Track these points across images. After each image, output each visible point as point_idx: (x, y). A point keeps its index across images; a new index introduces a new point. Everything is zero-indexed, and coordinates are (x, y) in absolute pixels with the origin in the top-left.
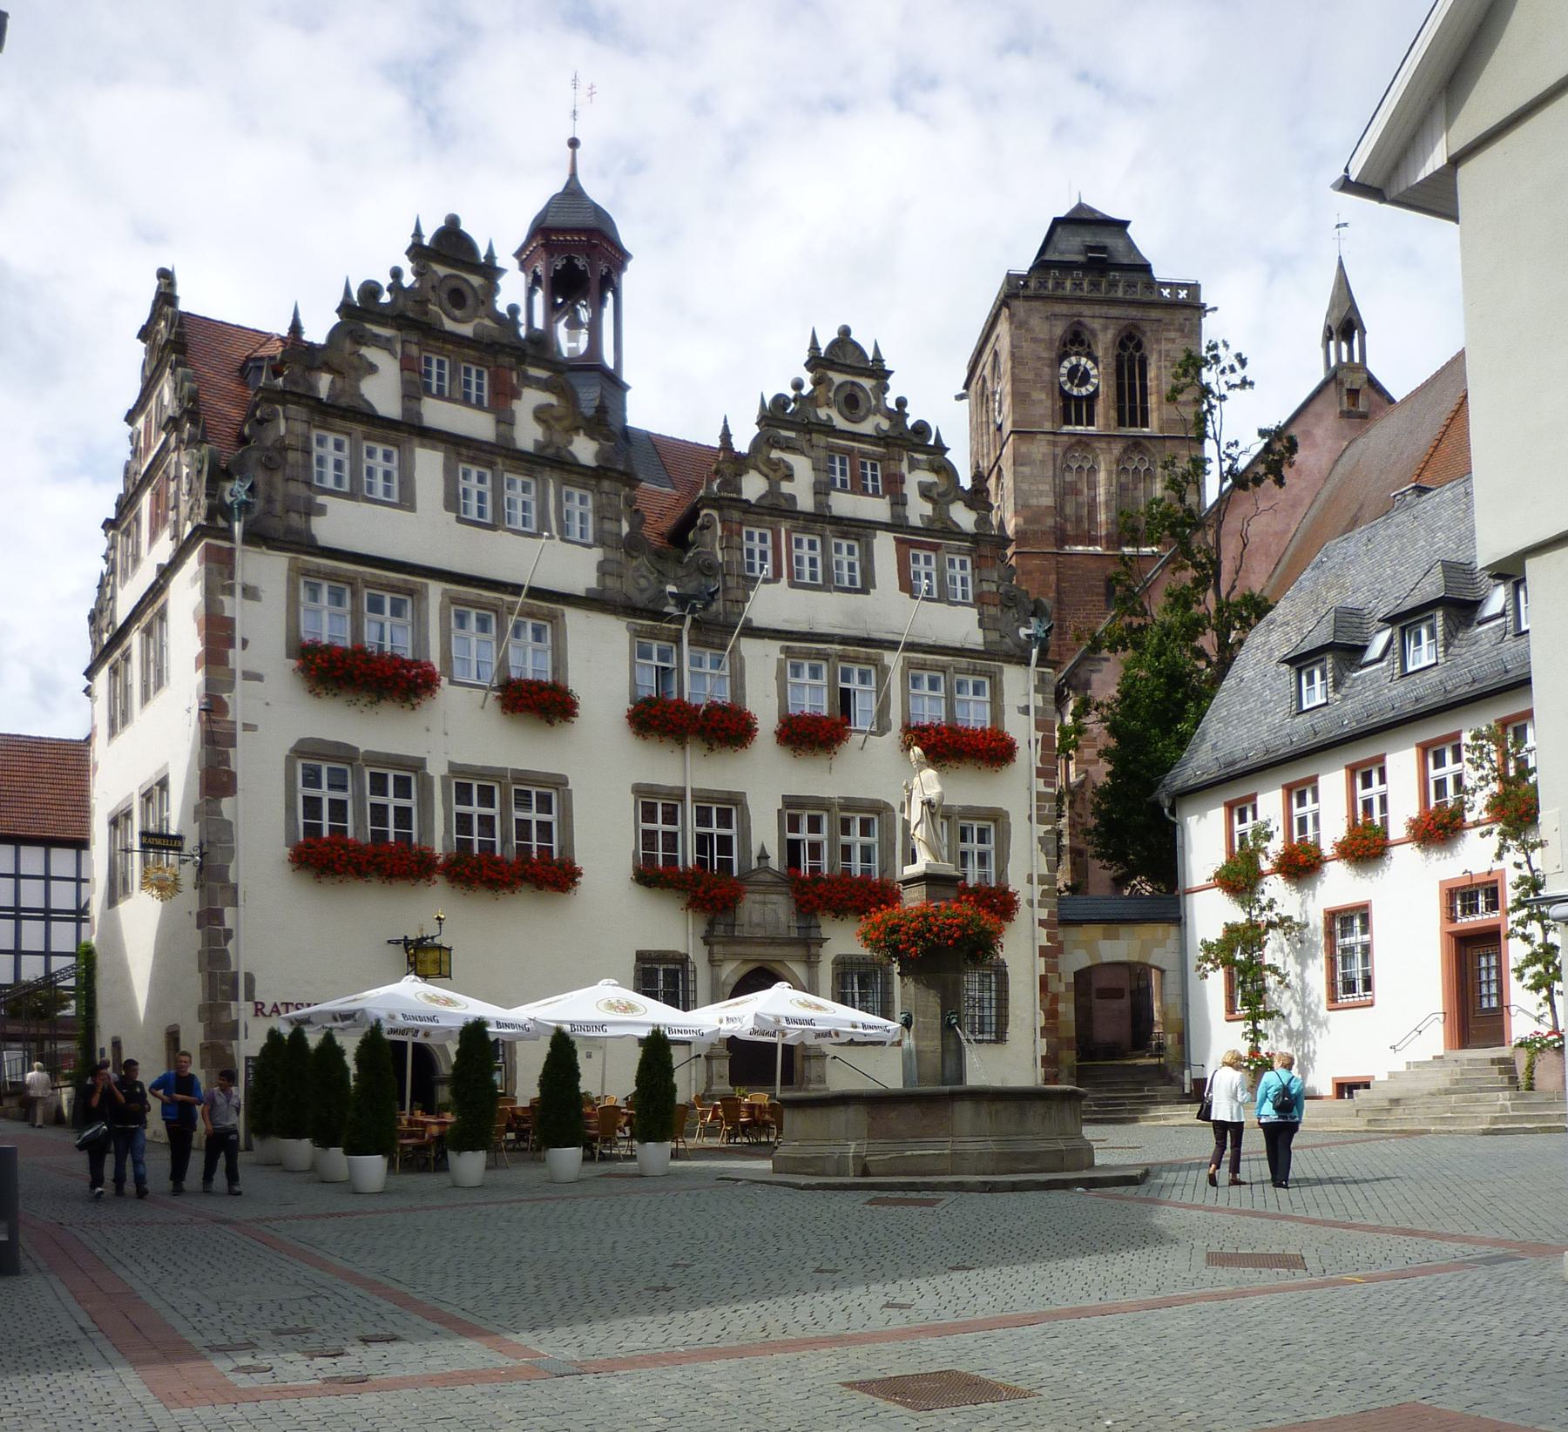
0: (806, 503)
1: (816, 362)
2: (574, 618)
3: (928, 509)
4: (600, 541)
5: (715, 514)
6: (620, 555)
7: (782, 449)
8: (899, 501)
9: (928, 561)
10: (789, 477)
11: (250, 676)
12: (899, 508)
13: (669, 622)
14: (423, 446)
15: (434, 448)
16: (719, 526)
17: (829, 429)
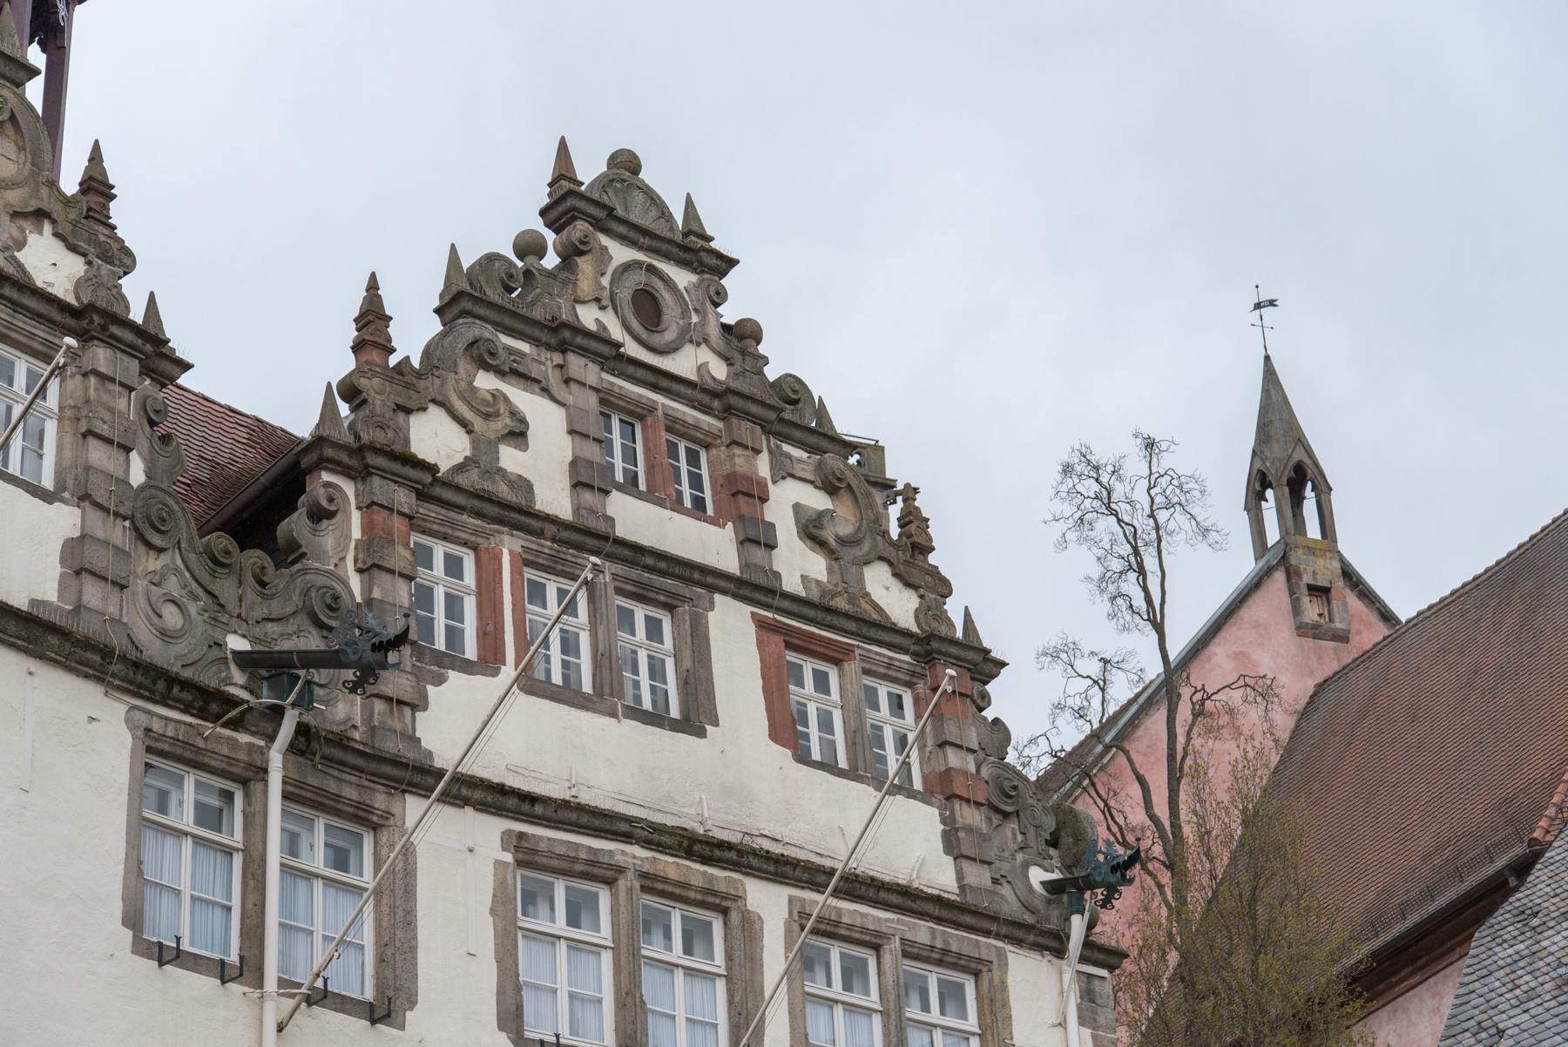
0: (555, 498)
1: (567, 204)
3: (817, 566)
4: (76, 488)
5: (348, 488)
6: (119, 533)
7: (500, 373)
8: (757, 538)
9: (822, 683)
10: (518, 435)
12: (758, 554)
13: (235, 724)
16: (356, 518)
17: (610, 356)
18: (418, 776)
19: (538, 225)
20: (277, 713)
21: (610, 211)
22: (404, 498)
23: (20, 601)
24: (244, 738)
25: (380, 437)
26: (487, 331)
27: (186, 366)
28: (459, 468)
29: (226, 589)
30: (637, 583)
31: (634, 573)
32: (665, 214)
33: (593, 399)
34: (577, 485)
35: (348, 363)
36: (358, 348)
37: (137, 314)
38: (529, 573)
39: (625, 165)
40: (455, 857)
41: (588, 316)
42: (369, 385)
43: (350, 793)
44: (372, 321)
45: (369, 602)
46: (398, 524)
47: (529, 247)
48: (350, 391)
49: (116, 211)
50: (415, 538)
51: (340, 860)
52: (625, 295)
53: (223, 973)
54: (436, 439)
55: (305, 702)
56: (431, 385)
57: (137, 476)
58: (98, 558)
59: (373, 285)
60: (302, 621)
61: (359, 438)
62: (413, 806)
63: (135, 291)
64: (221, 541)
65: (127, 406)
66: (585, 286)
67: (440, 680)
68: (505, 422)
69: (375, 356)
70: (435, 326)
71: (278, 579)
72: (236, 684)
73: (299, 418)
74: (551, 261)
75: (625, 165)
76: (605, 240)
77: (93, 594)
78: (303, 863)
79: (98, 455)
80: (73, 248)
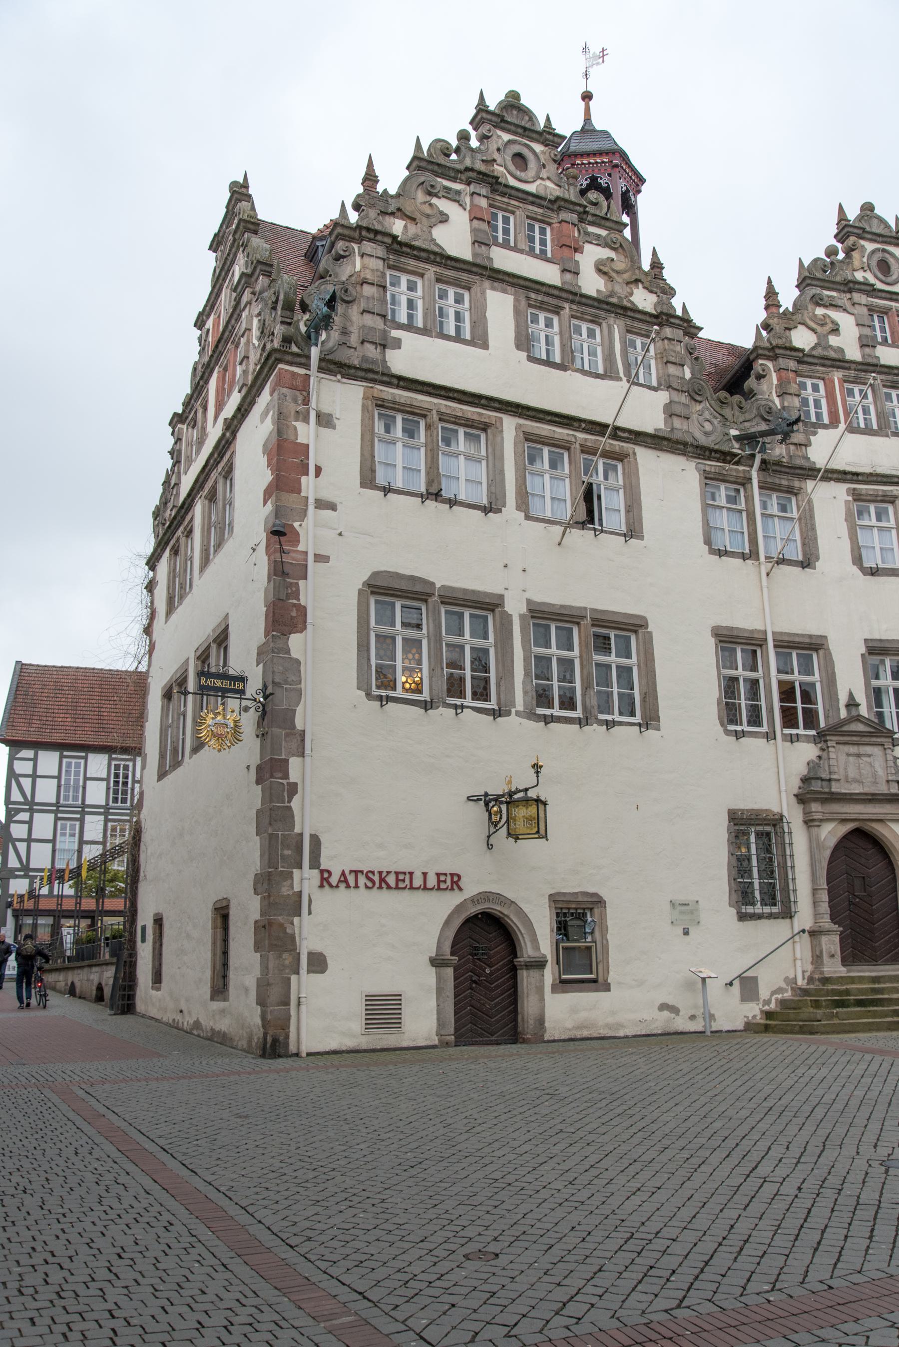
0: (854, 353)
2: (644, 457)
4: (666, 384)
5: (770, 364)
6: (684, 398)
7: (825, 306)
10: (836, 330)
11: (324, 505)
13: (738, 463)
14: (493, 288)
15: (504, 291)
16: (774, 375)
17: (870, 290)
18: (811, 472)
19: (834, 242)
20: (753, 456)
21: (864, 229)
22: (792, 364)
23: (650, 430)
24: (741, 468)
25: (780, 342)
26: (818, 291)
27: (700, 329)
28: (813, 348)
29: (727, 412)
30: (892, 382)
31: (890, 378)
32: (887, 226)
33: (865, 310)
34: (862, 346)
35: (763, 315)
36: (767, 308)
37: (679, 313)
38: (846, 385)
39: (868, 208)
40: (829, 502)
41: (859, 276)
42: (773, 322)
43: (785, 482)
44: (771, 294)
45: (783, 408)
46: (791, 375)
47: (831, 252)
48: (766, 326)
49: (666, 274)
50: (799, 379)
51: (783, 508)
52: (874, 263)
53: (743, 557)
54: (803, 339)
55: (763, 450)
56: (798, 317)
57: (688, 375)
58: (678, 409)
59: (769, 281)
60: (758, 419)
61: (773, 346)
62: (810, 484)
63: (677, 303)
64: (723, 394)
65: (680, 349)
66: (856, 263)
67: (815, 434)
68: (830, 326)
69: (774, 310)
70: (796, 293)
71: (746, 405)
72: (736, 448)
73: (747, 341)
74: (841, 256)
75: (868, 208)
76: (862, 242)
77: (677, 423)
78: (769, 512)
79: (672, 369)
80: (651, 292)
